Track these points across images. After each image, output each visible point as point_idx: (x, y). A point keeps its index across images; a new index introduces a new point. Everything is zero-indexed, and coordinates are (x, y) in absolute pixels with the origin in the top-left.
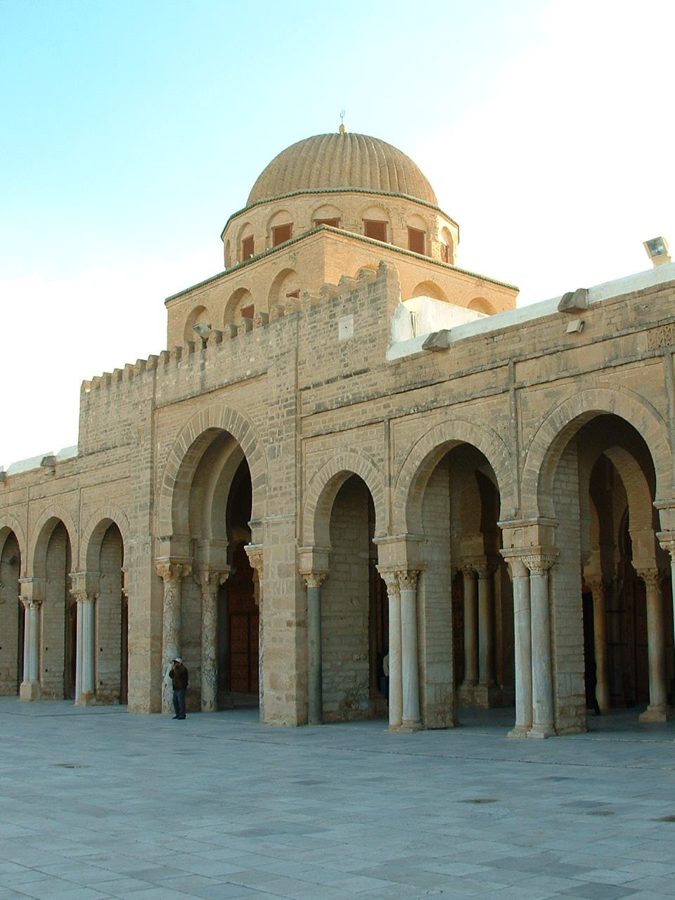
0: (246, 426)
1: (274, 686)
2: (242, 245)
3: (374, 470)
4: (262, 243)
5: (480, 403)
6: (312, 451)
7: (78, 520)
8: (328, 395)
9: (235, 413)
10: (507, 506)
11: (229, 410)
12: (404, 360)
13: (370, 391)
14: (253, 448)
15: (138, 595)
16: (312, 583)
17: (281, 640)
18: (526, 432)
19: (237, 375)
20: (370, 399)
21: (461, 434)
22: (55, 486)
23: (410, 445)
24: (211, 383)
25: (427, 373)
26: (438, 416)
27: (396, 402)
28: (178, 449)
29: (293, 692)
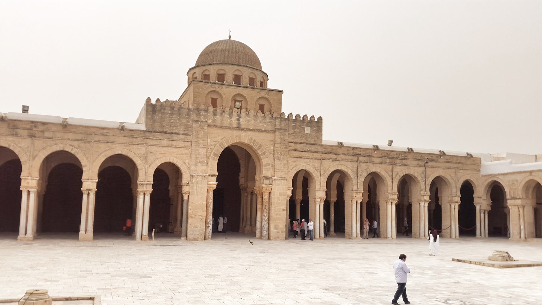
0: (261, 146)
1: (276, 228)
2: (233, 76)
3: (316, 172)
4: (245, 81)
5: (349, 163)
6: (292, 162)
7: (146, 159)
8: (299, 147)
9: (255, 141)
10: (355, 188)
11: (251, 139)
12: (328, 146)
13: (316, 150)
14: (264, 153)
15: (197, 195)
16: (289, 199)
17: (280, 215)
18: (360, 172)
19: (257, 128)
20: (316, 152)
21: (343, 168)
22: (121, 139)
23: (328, 168)
24: (242, 127)
25: (335, 151)
26: (337, 162)
27: (324, 156)
28: (221, 144)
29: (285, 230)
